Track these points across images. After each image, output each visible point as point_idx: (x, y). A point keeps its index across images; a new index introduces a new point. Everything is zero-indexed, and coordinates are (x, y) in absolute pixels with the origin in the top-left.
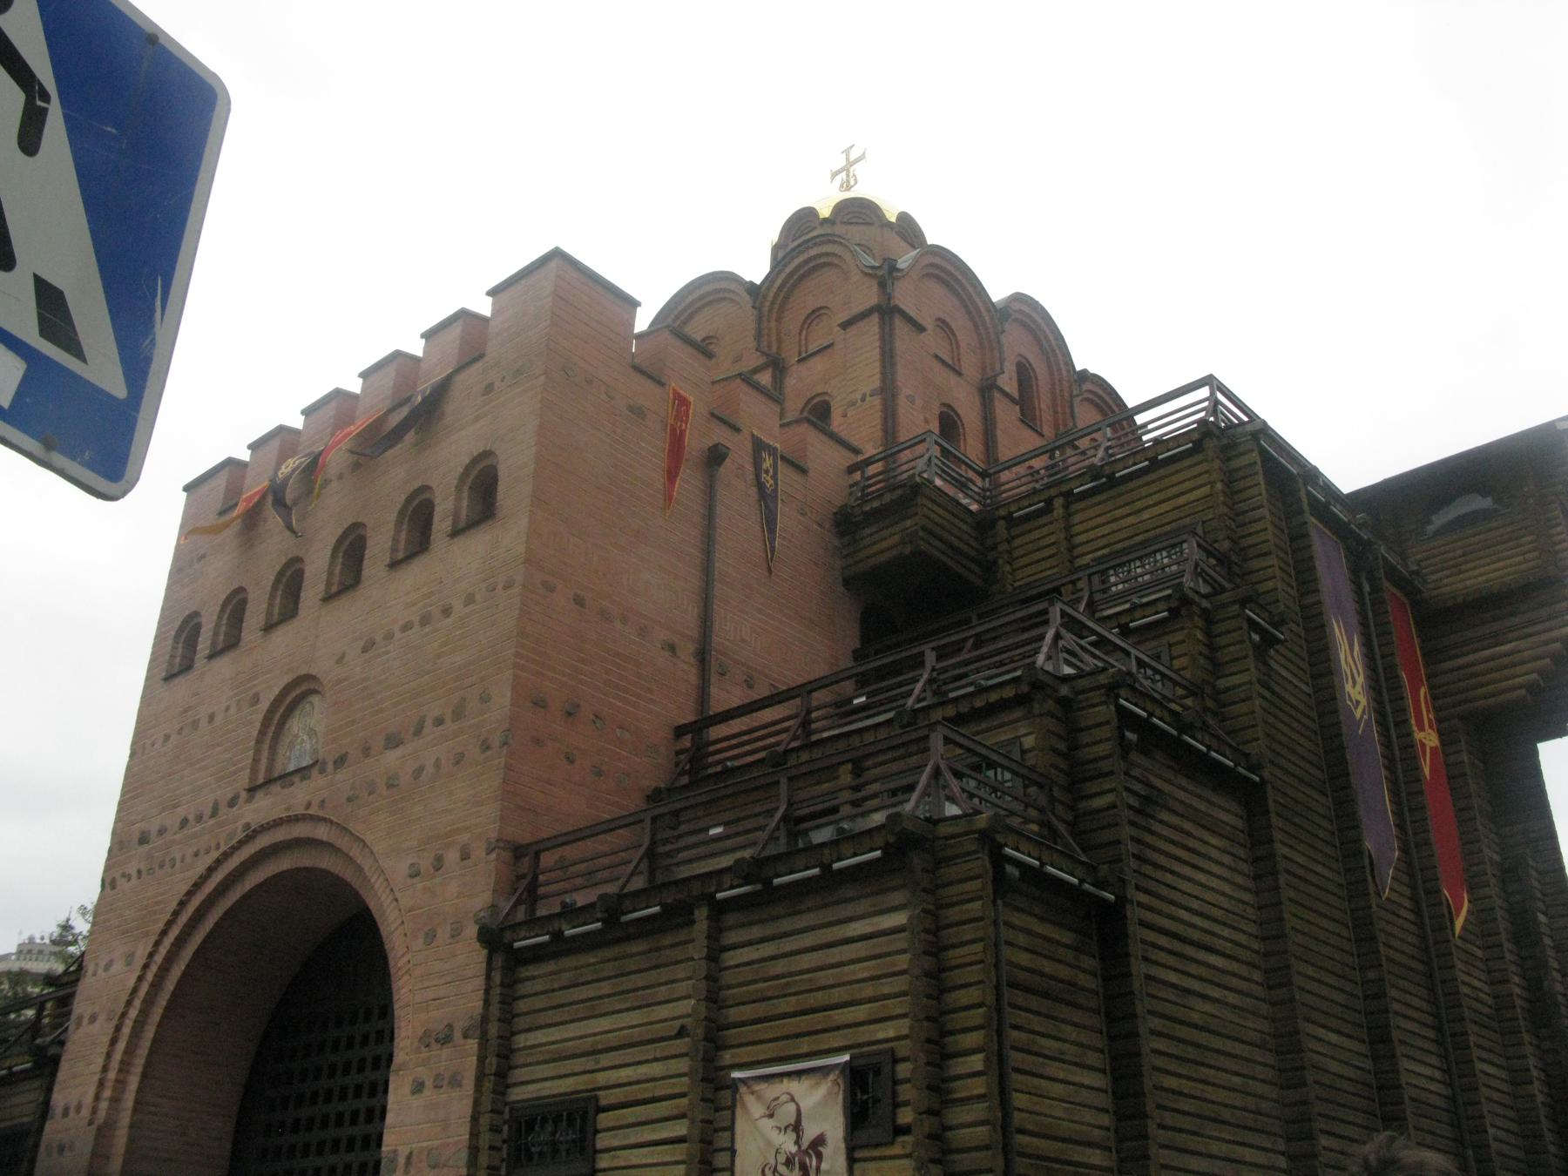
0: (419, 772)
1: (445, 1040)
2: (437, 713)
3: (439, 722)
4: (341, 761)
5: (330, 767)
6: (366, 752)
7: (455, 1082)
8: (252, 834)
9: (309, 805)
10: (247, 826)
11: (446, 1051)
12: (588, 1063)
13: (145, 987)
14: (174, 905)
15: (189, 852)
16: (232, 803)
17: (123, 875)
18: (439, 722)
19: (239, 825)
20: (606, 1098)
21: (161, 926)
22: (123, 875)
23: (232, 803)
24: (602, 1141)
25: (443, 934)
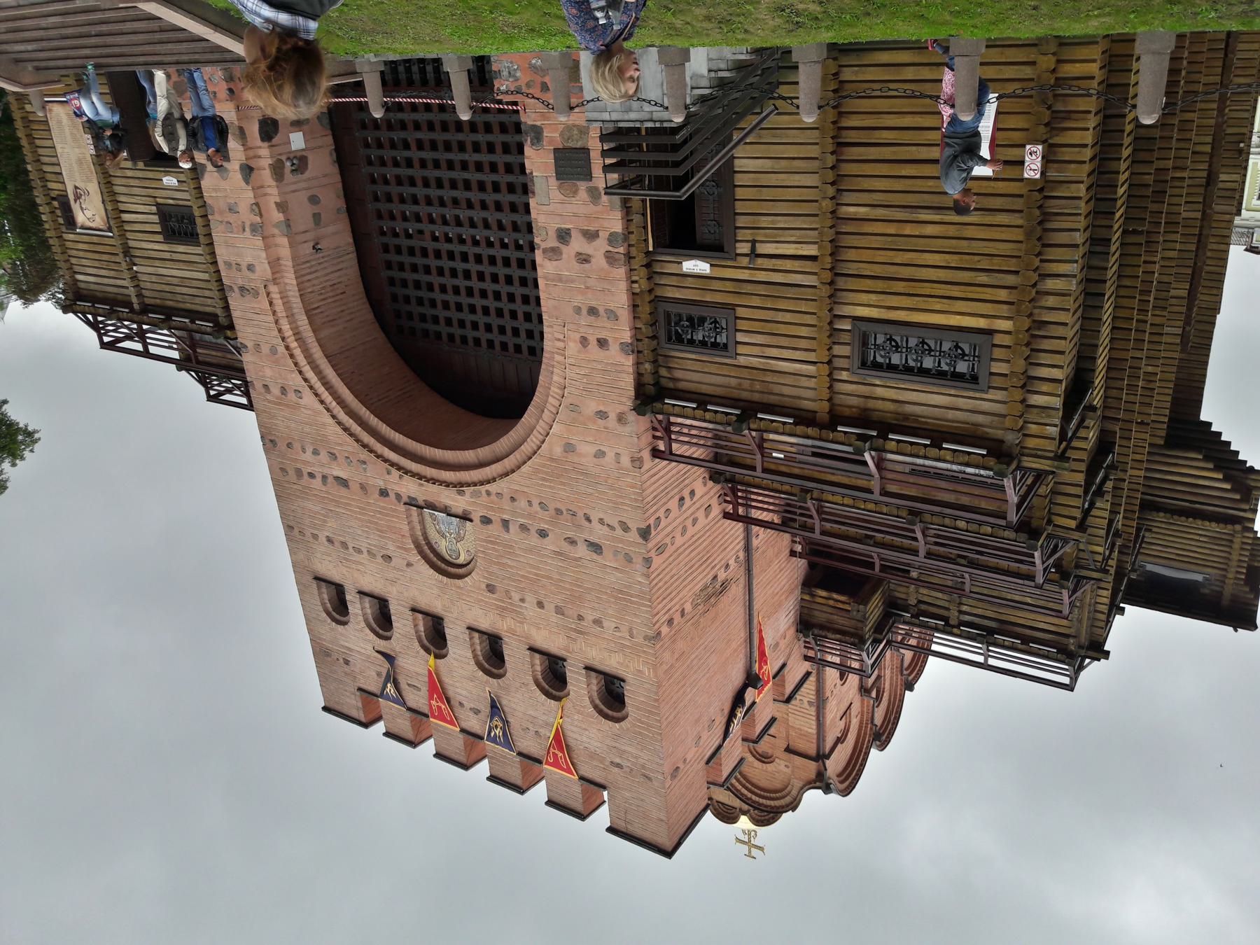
1: (242, 289)
3: (311, 475)
4: (384, 493)
5: (392, 496)
7: (228, 264)
8: (459, 485)
11: (240, 282)
12: (175, 256)
14: (524, 469)
15: (522, 503)
16: (486, 521)
17: (612, 528)
19: (467, 497)
20: (160, 238)
22: (612, 528)
23: (486, 521)
24: (155, 218)
25: (265, 349)
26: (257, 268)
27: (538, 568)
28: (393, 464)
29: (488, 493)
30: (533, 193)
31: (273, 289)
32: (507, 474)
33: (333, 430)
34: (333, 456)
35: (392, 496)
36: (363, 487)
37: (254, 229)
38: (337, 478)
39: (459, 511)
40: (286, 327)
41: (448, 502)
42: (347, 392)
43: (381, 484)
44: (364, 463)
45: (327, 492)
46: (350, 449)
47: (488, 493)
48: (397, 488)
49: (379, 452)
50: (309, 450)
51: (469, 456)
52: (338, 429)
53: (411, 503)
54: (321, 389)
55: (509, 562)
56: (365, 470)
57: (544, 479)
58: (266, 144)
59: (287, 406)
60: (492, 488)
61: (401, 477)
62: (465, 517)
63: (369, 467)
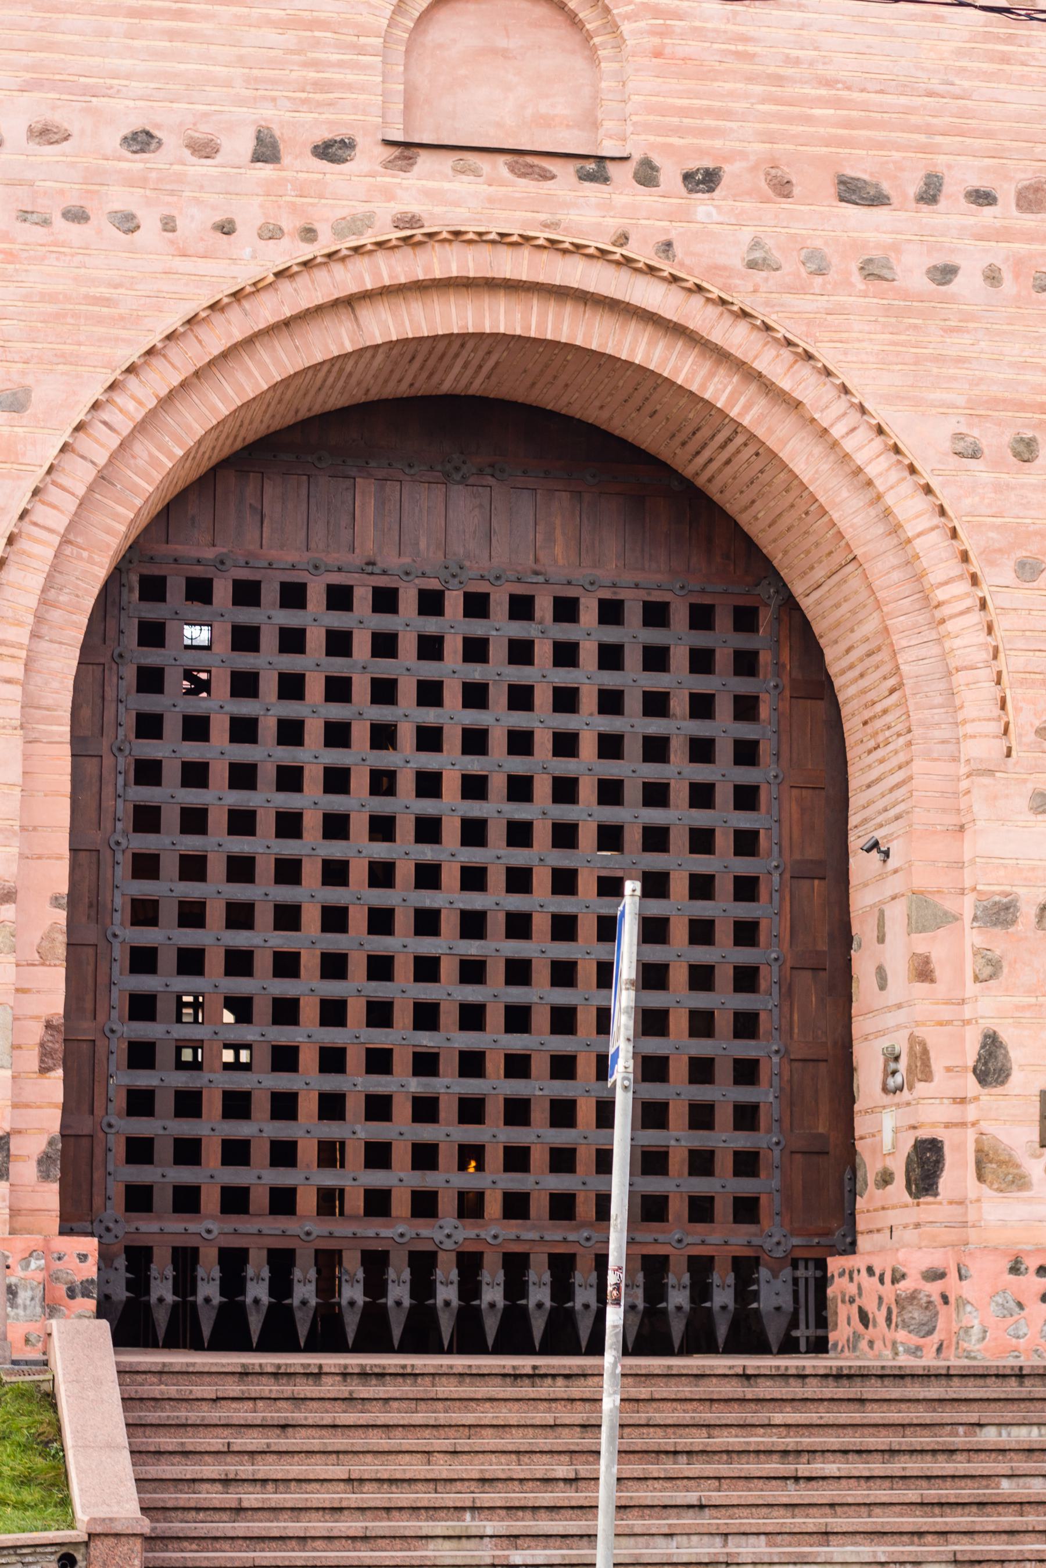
0: (945, 273)
2: (975, 182)
3: (983, 198)
4: (704, 180)
5: (670, 176)
6: (783, 188)
8: (413, 237)
9: (623, 239)
10: (413, 221)
13: (78, 476)
14: (174, 320)
15: (194, 222)
16: (333, 151)
18: (983, 198)
21: (133, 354)
23: (333, 151)
26: (1021, 802)
27: (172, 35)
28: (651, 270)
29: (309, 234)
30: (49, 1026)
31: (983, 747)
32: (237, 295)
33: (859, 347)
34: (874, 271)
35: (670, 176)
36: (783, 188)
37: (1000, 913)
38: (878, 200)
39: (425, 161)
40: (966, 638)
41: (463, 186)
42: (801, 467)
43: (705, 208)
44: (752, 265)
45: (923, 149)
46: (806, 304)
47: (309, 234)
48: (645, 197)
49: (697, 300)
50: (968, 283)
51: (383, 325)
52: (826, 354)
53: (595, 168)
54: (879, 467)
55: (272, 36)
56: (756, 244)
57: (106, 302)
58: (924, 1134)
59: (1022, 406)
60: (290, 251)
61: (623, 239)
62: (406, 150)
63: (735, 258)
